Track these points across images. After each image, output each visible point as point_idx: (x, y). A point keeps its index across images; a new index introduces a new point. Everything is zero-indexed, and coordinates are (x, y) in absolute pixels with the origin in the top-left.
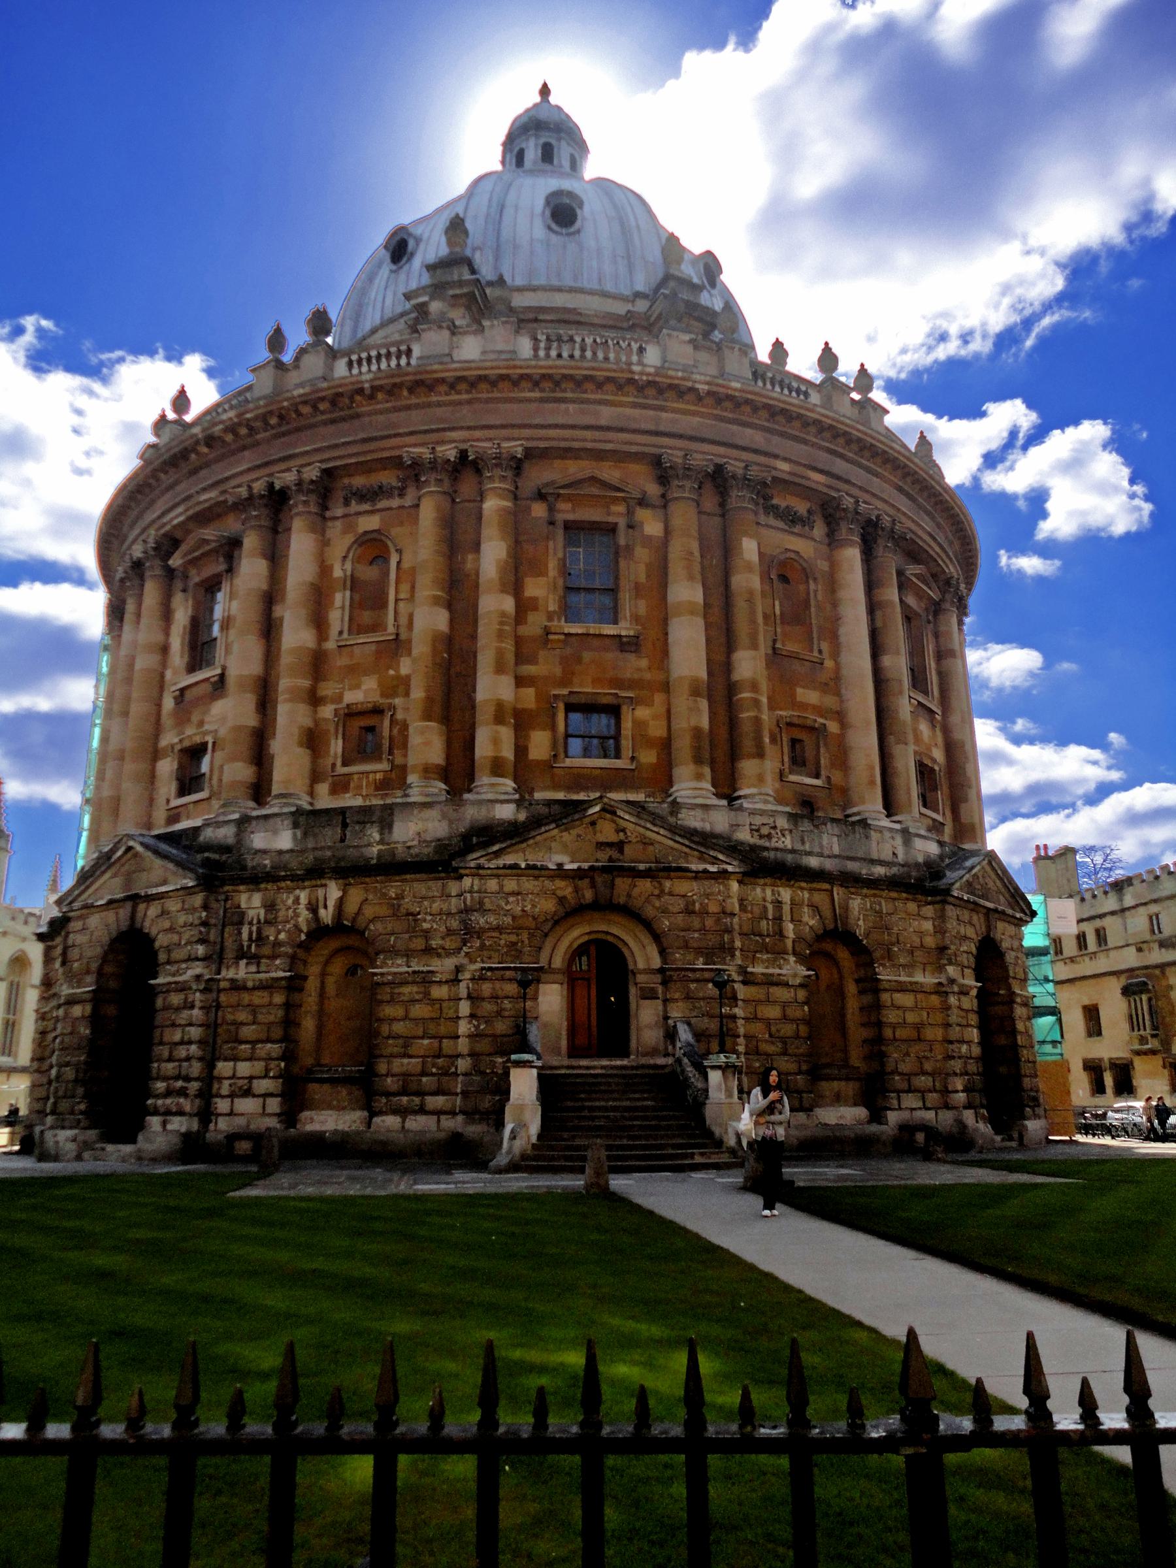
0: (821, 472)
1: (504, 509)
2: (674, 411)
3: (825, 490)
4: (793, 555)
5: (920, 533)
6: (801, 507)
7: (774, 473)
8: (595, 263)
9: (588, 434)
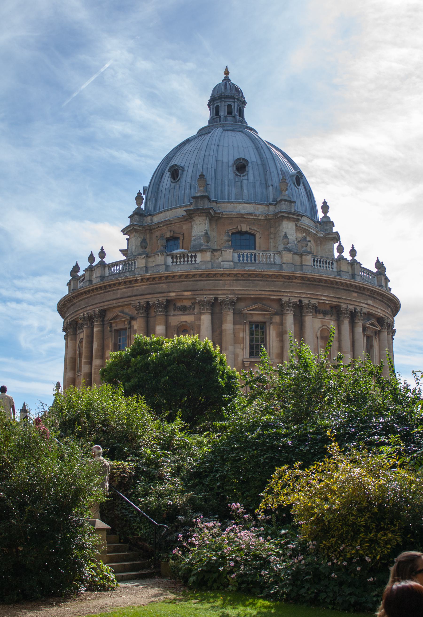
0: (189, 291)
1: (98, 331)
2: (136, 286)
3: (192, 297)
4: (184, 323)
5: (251, 293)
6: (187, 303)
7: (169, 298)
8: (183, 192)
9: (114, 302)
